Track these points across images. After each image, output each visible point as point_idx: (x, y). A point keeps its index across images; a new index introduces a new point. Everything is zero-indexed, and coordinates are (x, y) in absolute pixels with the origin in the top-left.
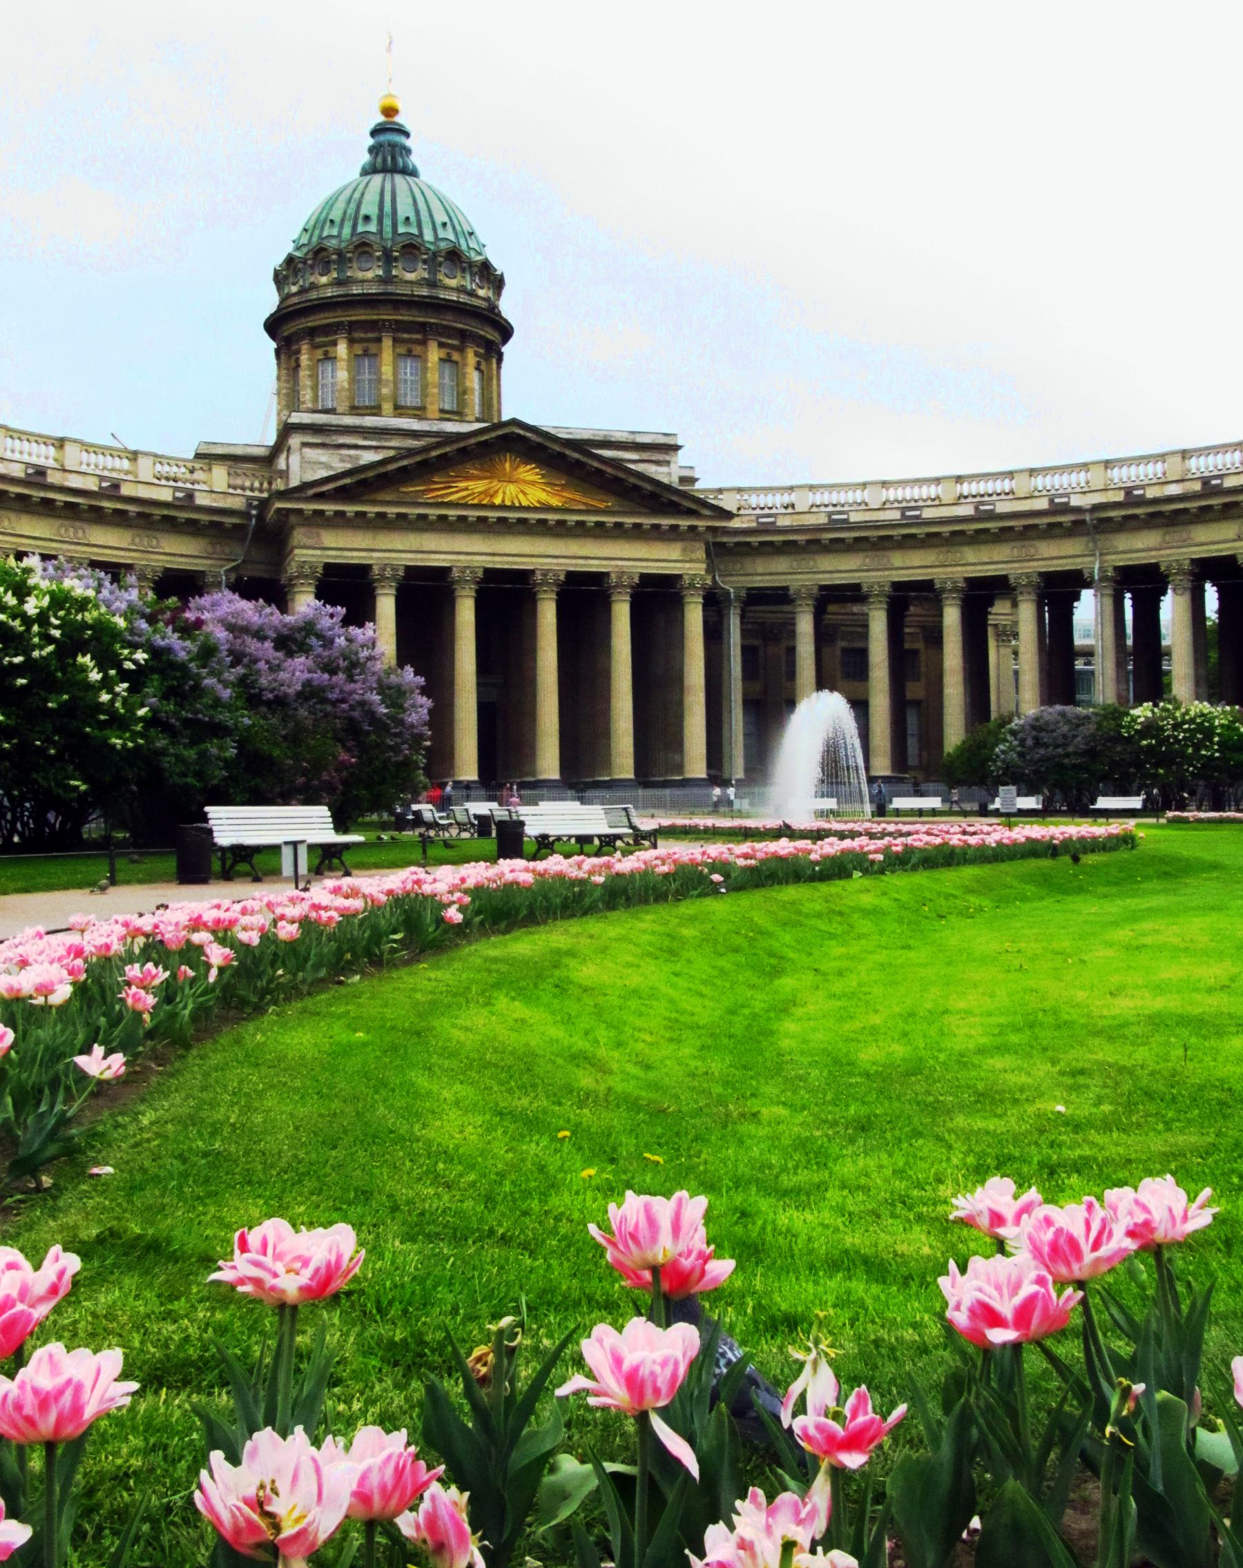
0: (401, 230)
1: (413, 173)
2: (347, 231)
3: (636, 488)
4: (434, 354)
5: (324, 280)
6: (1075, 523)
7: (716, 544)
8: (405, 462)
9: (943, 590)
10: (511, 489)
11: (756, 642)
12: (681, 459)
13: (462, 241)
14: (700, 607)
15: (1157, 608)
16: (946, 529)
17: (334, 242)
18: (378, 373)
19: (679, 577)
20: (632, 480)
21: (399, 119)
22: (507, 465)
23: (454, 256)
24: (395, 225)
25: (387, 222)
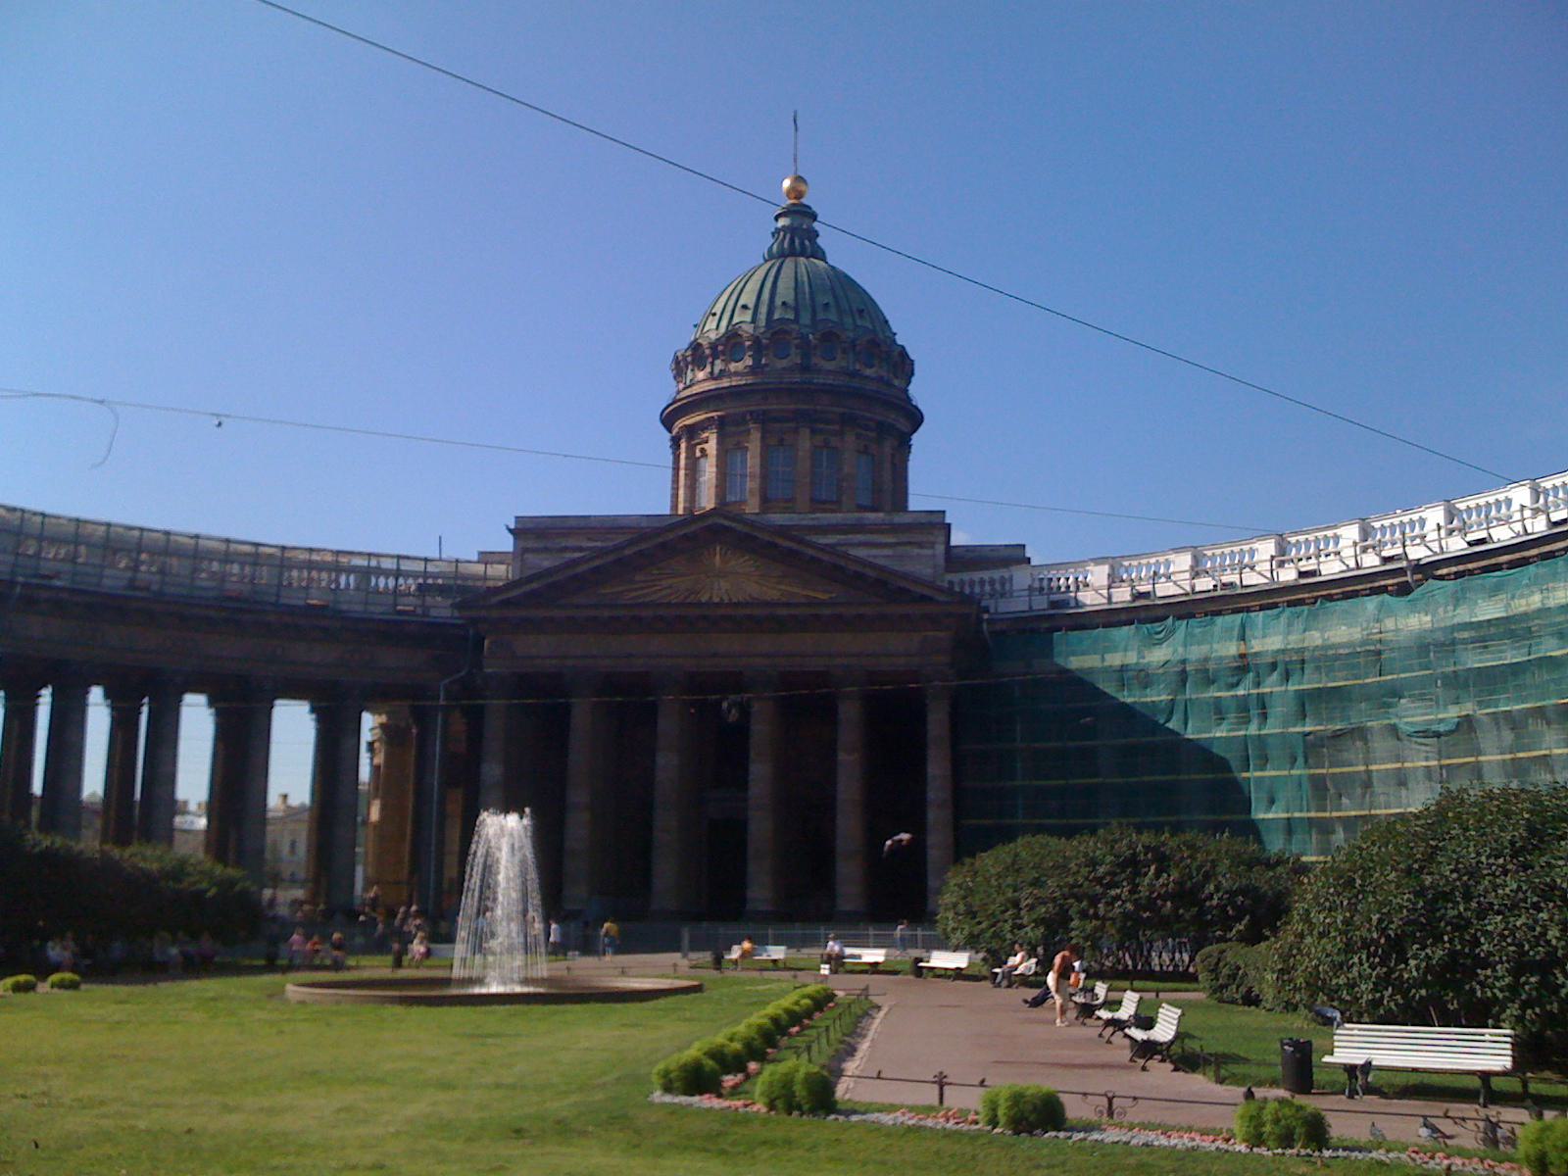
0: (776, 316)
1: (819, 254)
2: (724, 323)
3: (858, 575)
4: (805, 442)
5: (701, 375)
8: (597, 563)
10: (724, 585)
12: (958, 539)
13: (848, 320)
17: (713, 336)
18: (744, 462)
20: (853, 567)
21: (804, 201)
22: (718, 557)
23: (829, 337)
24: (770, 312)
25: (763, 309)
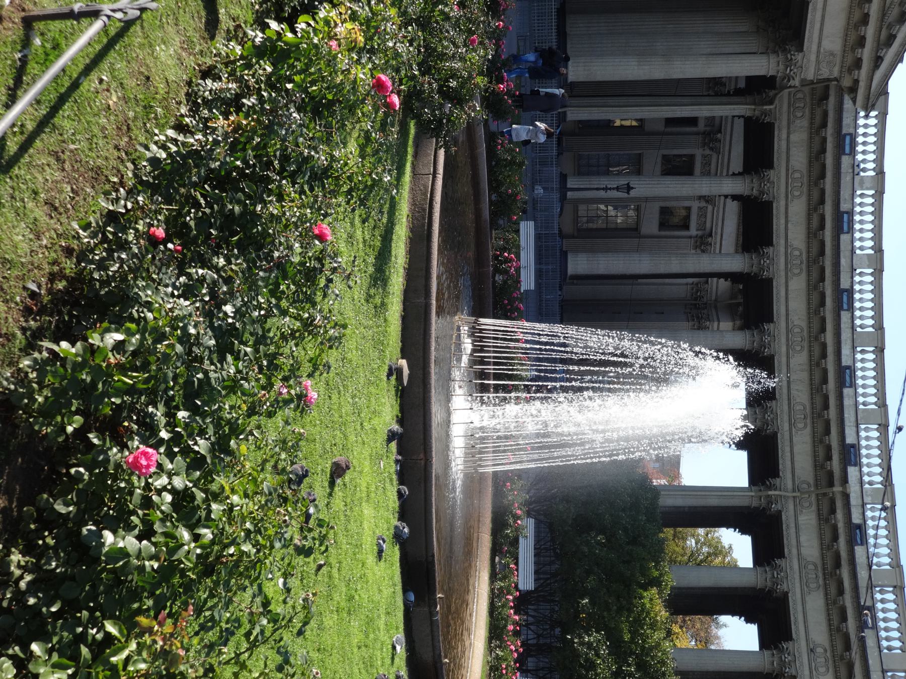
6: (831, 474)
7: (827, 88)
9: (762, 332)
11: (701, 126)
14: (762, 72)
15: (728, 526)
16: (829, 337)
19: (800, 48)
